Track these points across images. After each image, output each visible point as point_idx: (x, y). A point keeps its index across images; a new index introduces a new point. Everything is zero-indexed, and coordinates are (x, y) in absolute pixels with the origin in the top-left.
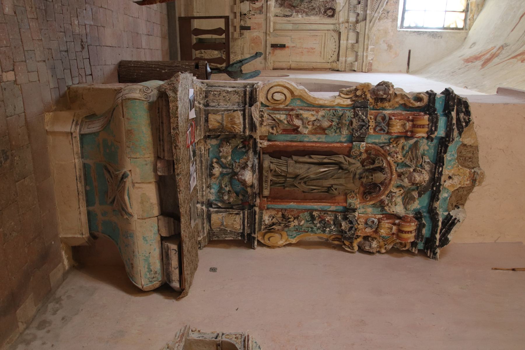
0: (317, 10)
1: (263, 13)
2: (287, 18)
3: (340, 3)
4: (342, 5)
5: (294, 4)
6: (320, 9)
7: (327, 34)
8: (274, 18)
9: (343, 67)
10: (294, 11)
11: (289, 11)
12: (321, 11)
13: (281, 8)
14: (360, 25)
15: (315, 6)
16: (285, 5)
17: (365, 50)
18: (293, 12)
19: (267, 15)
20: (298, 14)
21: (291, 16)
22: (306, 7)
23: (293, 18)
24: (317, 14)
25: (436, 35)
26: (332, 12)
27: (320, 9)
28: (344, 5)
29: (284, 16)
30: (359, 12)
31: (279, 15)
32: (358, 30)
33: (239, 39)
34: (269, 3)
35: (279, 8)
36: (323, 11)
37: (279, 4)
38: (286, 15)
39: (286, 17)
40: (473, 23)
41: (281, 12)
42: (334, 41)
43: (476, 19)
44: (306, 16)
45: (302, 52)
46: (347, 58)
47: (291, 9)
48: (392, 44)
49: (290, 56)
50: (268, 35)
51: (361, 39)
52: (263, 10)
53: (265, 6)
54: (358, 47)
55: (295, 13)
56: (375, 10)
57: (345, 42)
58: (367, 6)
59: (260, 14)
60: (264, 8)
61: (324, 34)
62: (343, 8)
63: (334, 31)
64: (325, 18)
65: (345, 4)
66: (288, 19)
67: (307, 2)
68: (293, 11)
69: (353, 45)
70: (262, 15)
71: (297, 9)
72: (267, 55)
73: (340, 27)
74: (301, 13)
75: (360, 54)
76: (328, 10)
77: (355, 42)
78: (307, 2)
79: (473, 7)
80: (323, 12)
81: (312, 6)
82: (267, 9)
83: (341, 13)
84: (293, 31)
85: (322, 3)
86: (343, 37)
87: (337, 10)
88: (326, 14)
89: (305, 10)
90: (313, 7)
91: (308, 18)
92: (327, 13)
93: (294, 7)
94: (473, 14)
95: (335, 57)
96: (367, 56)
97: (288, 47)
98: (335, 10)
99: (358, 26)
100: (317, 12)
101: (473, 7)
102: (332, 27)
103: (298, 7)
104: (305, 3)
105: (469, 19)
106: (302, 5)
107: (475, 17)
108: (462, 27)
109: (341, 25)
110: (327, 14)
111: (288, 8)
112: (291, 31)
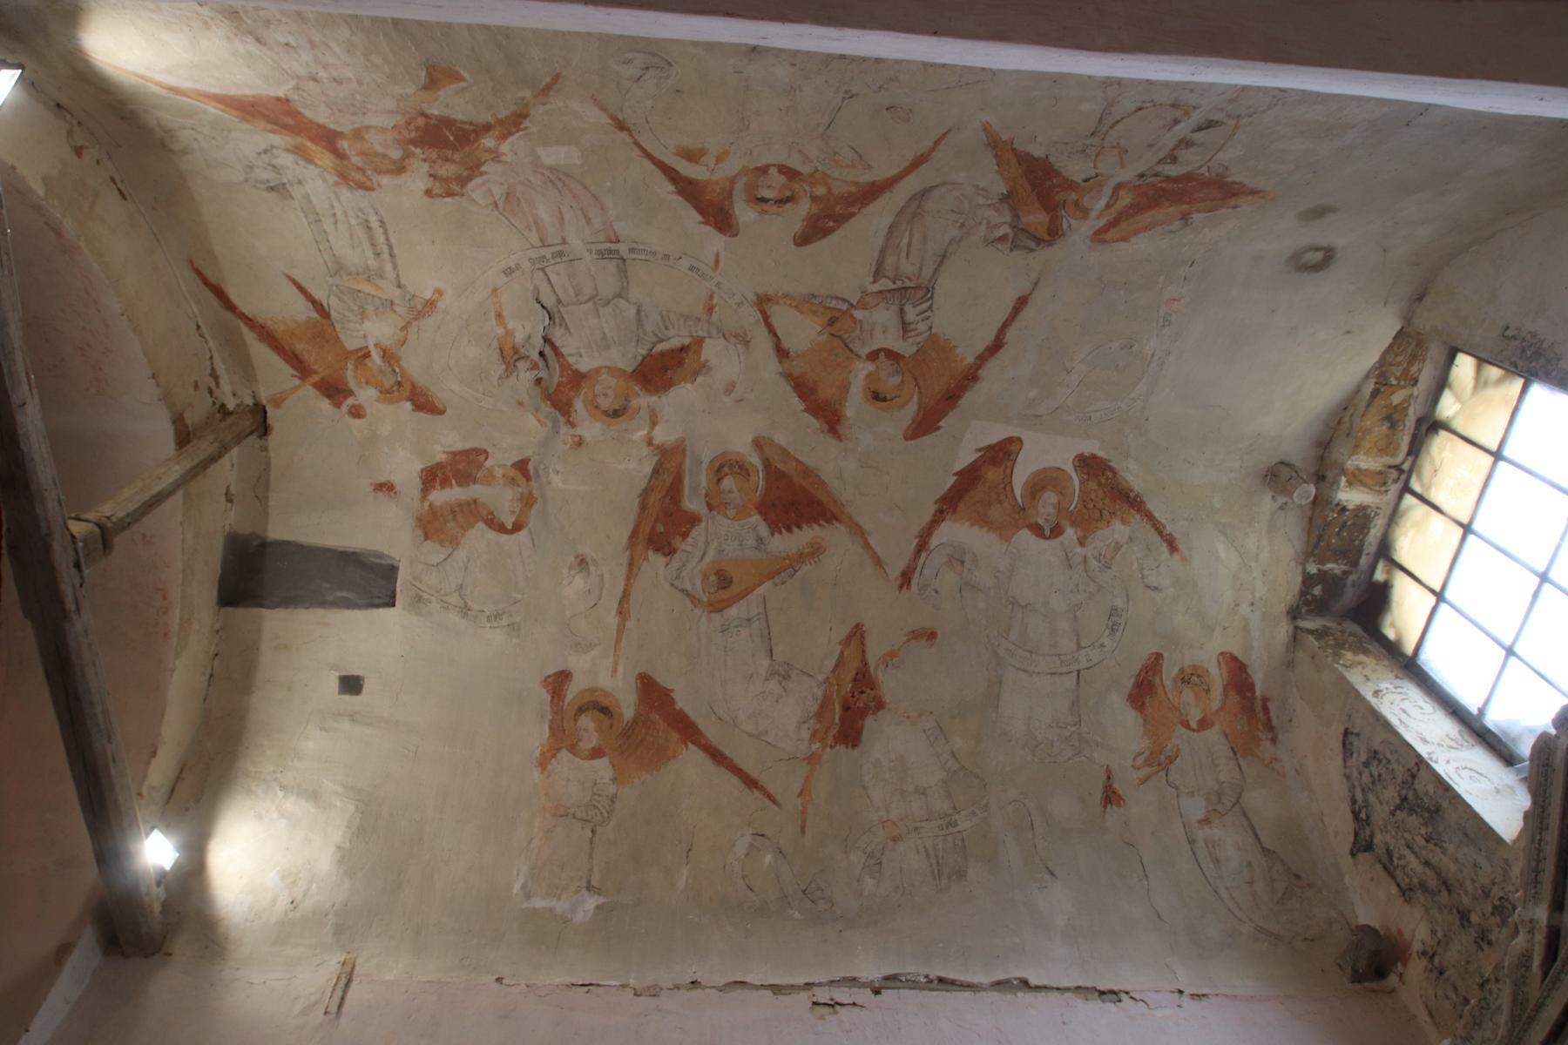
25: (1523, 350)
43: (1367, 377)
94: (1380, 402)
105: (1415, 382)
107: (1370, 386)
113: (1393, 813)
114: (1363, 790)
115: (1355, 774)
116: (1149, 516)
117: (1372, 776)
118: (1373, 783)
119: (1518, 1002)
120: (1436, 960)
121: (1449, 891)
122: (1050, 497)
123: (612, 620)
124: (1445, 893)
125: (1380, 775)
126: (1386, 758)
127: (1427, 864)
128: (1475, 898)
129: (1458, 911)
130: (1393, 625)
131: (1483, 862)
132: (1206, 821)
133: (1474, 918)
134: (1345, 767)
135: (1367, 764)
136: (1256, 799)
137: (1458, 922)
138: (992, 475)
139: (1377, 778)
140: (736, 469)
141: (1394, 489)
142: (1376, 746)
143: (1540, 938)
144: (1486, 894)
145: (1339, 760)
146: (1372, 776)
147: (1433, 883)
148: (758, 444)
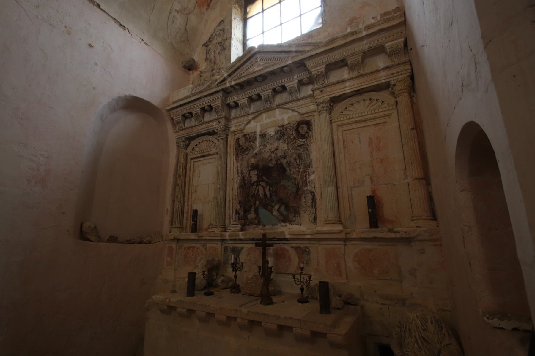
0: (300, 151)
1: (307, 247)
2: (318, 201)
3: (289, 118)
4: (290, 113)
5: (294, 190)
6: (299, 146)
7: (339, 123)
8: (319, 224)
9: (401, 68)
10: (305, 189)
11: (305, 197)
14: (313, 67)
15: (294, 155)
17: (355, 37)
18: (307, 190)
19: (309, 239)
20: (309, 182)
21: (312, 193)
22: (297, 169)
23: (317, 189)
24: (308, 150)
26: (302, 126)
27: (299, 146)
28: (290, 111)
29: (315, 205)
31: (313, 215)
32: (322, 68)
33: (362, 307)
34: (287, 236)
37: (295, 216)
38: (313, 201)
39: (316, 202)
41: (308, 212)
42: (350, 109)
44: (312, 167)
45: (382, 161)
46: (379, 69)
48: (348, 19)
49: (394, 185)
50: (349, 236)
51: (336, 56)
52: (302, 246)
53: (295, 244)
54: (353, 54)
55: (308, 187)
57: (347, 84)
59: (309, 253)
60: (297, 245)
61: (341, 129)
63: (330, 111)
64: (313, 134)
65: (288, 109)
66: (318, 197)
68: (304, 191)
69: (352, 68)
70: (310, 248)
71: (300, 184)
72: (398, 236)
73: (322, 100)
74: (307, 177)
75: (365, 45)
77: (346, 68)
78: (290, 169)
80: (304, 140)
81: (295, 159)
82: (298, 239)
83: (303, 111)
84: (340, 185)
85: (290, 144)
86: (338, 91)
87: (298, 118)
88: (307, 135)
89: (302, 170)
90: (297, 158)
91: (314, 164)
92: (304, 133)
95: (384, 95)
96: (368, 27)
97: (374, 191)
99: (316, 72)
102: (324, 117)
103: (298, 183)
104: (292, 173)
106: (295, 176)
109: (318, 101)
110: (307, 132)
112: (340, 191)
113: (217, 43)
114: (215, 35)
115: (217, 30)
117: (219, 33)
118: (219, 35)
119: (209, 86)
120: (201, 74)
121: (214, 64)
124: (213, 64)
125: (221, 34)
126: (225, 32)
127: (215, 57)
128: (217, 68)
129: (213, 69)
130: (250, 8)
131: (224, 63)
132: (177, 12)
133: (214, 71)
134: (216, 27)
135: (220, 30)
136: (193, 18)
137: (211, 70)
139: (220, 34)
142: (225, 28)
143: (222, 78)
144: (220, 69)
145: (216, 25)
146: (219, 33)
147: (213, 61)
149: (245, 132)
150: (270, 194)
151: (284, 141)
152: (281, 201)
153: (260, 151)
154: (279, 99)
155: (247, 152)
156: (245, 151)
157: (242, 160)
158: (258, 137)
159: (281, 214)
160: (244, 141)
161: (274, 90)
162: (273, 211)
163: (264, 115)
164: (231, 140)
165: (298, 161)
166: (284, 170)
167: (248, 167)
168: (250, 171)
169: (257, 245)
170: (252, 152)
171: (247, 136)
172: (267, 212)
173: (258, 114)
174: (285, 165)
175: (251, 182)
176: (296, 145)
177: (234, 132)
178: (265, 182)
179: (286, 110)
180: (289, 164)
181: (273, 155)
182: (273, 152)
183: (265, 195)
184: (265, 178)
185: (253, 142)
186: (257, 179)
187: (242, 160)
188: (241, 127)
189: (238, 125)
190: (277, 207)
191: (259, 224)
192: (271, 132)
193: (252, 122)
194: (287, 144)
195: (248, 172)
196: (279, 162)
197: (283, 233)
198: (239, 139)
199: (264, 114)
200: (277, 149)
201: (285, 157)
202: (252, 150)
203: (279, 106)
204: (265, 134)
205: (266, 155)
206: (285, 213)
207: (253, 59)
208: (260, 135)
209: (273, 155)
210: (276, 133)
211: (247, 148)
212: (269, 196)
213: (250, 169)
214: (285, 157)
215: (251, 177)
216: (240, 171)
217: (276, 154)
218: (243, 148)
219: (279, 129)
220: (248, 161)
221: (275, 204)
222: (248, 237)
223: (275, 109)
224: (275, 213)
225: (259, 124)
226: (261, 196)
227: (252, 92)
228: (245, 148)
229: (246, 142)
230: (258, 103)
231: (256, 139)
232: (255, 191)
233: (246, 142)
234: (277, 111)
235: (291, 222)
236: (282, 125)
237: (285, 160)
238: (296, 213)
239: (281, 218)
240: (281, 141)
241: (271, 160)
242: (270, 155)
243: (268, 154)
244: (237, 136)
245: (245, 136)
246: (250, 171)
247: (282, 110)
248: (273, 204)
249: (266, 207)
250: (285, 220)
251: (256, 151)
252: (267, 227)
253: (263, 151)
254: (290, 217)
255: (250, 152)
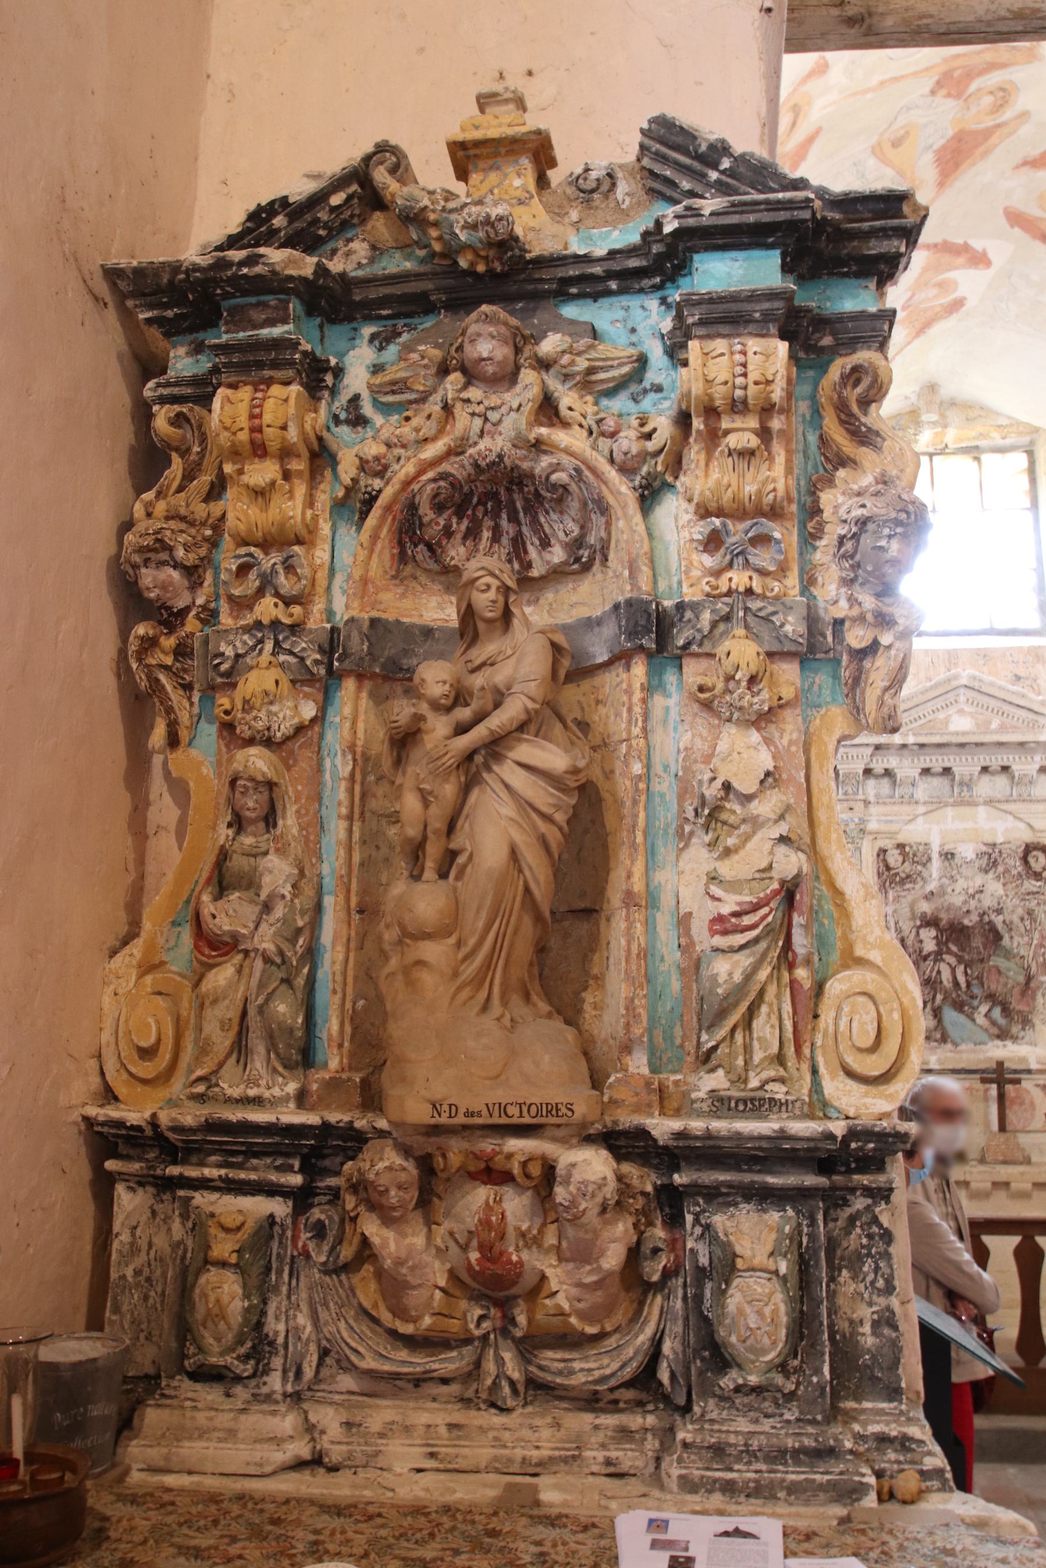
4: (1010, 822)
5: (1021, 979)
12: (1035, 890)
13: (1037, 1021)
15: (1020, 911)
16: (1026, 1009)
22: (1026, 939)
26: (1034, 853)
28: (1010, 818)
30: (1037, 767)
34: (1034, 1066)
35: (1037, 1028)
36: (1034, 882)
37: (1023, 1029)
40: (1019, 423)
43: (1009, 418)
47: (1038, 988)
56: (1031, 716)
58: (1022, 744)
62: (1020, 819)
67: (1012, 937)
71: (1034, 969)
76: (1030, 868)
78: (1012, 937)
79: (969, 435)
80: (1039, 884)
81: (1022, 919)
85: (1009, 886)
87: (1028, 837)
89: (1035, 942)
93: (1029, 979)
98: (1027, 846)
100: (1039, 904)
101: (973, 434)
103: (1029, 966)
104: (1015, 944)
105: (1004, 438)
106: (1022, 952)
107: (1004, 422)
108: (1024, 456)
111: (1034, 998)
116: (909, 343)
122: (932, 292)
123: (874, 81)
138: (960, 260)
140: (999, 103)
141: (931, 450)
148: (1024, 116)
149: (901, 839)
150: (968, 982)
151: (998, 878)
152: (991, 997)
153: (942, 891)
154: (987, 786)
155: (908, 886)
156: (902, 882)
157: (897, 899)
158: (935, 856)
159: (994, 1023)
160: (900, 859)
161: (985, 769)
162: (976, 1015)
163: (950, 811)
164: (868, 851)
165: (1027, 923)
166: (998, 937)
167: (913, 918)
168: (919, 928)
169: (984, 1081)
170: (922, 887)
171: (907, 849)
172: (961, 1018)
173: (937, 804)
174: (1000, 927)
175: (921, 951)
176: (1023, 890)
177: (876, 835)
178: (956, 955)
179: (1003, 815)
180: (1009, 926)
181: (973, 904)
182: (973, 896)
183: (956, 983)
184: (954, 948)
185: (924, 865)
186: (935, 948)
187: (897, 899)
188: (894, 827)
189: (887, 822)
190: (984, 1009)
191: (944, 1039)
192: (967, 851)
193: (920, 820)
194: (1004, 885)
195: (914, 931)
196: (986, 919)
197: (1024, 1060)
198: (885, 851)
199: (949, 809)
200: (981, 892)
201: (999, 911)
202: (921, 883)
203: (990, 802)
204: (953, 854)
205: (957, 900)
206: (1002, 1021)
207: (951, 696)
208: (941, 855)
209: (973, 904)
210: (980, 855)
211: (908, 876)
212: (963, 985)
213: (918, 923)
214: (999, 911)
215: (921, 941)
216: (892, 924)
217: (979, 901)
218: (897, 874)
219: (984, 849)
220: (912, 907)
221: (980, 1003)
222: (951, 1067)
223: (975, 804)
224: (980, 1019)
225: (936, 829)
226: (945, 983)
227: (937, 762)
228: (903, 875)
229: (904, 862)
230: (936, 782)
231: (929, 859)
232: (931, 972)
233: (904, 862)
234: (981, 809)
235: (1015, 1039)
236: (990, 841)
237: (1001, 918)
238: (1026, 1022)
239: (995, 1031)
240: (991, 875)
241: (968, 912)
242: (965, 902)
243: (962, 898)
244: (882, 843)
245: (901, 846)
246: (919, 928)
247: (993, 810)
248: (975, 1003)
249: (959, 1006)
250: (1003, 1035)
251: (932, 886)
252: (963, 1047)
253: (949, 890)
254: (1015, 1029)
255: (918, 887)
